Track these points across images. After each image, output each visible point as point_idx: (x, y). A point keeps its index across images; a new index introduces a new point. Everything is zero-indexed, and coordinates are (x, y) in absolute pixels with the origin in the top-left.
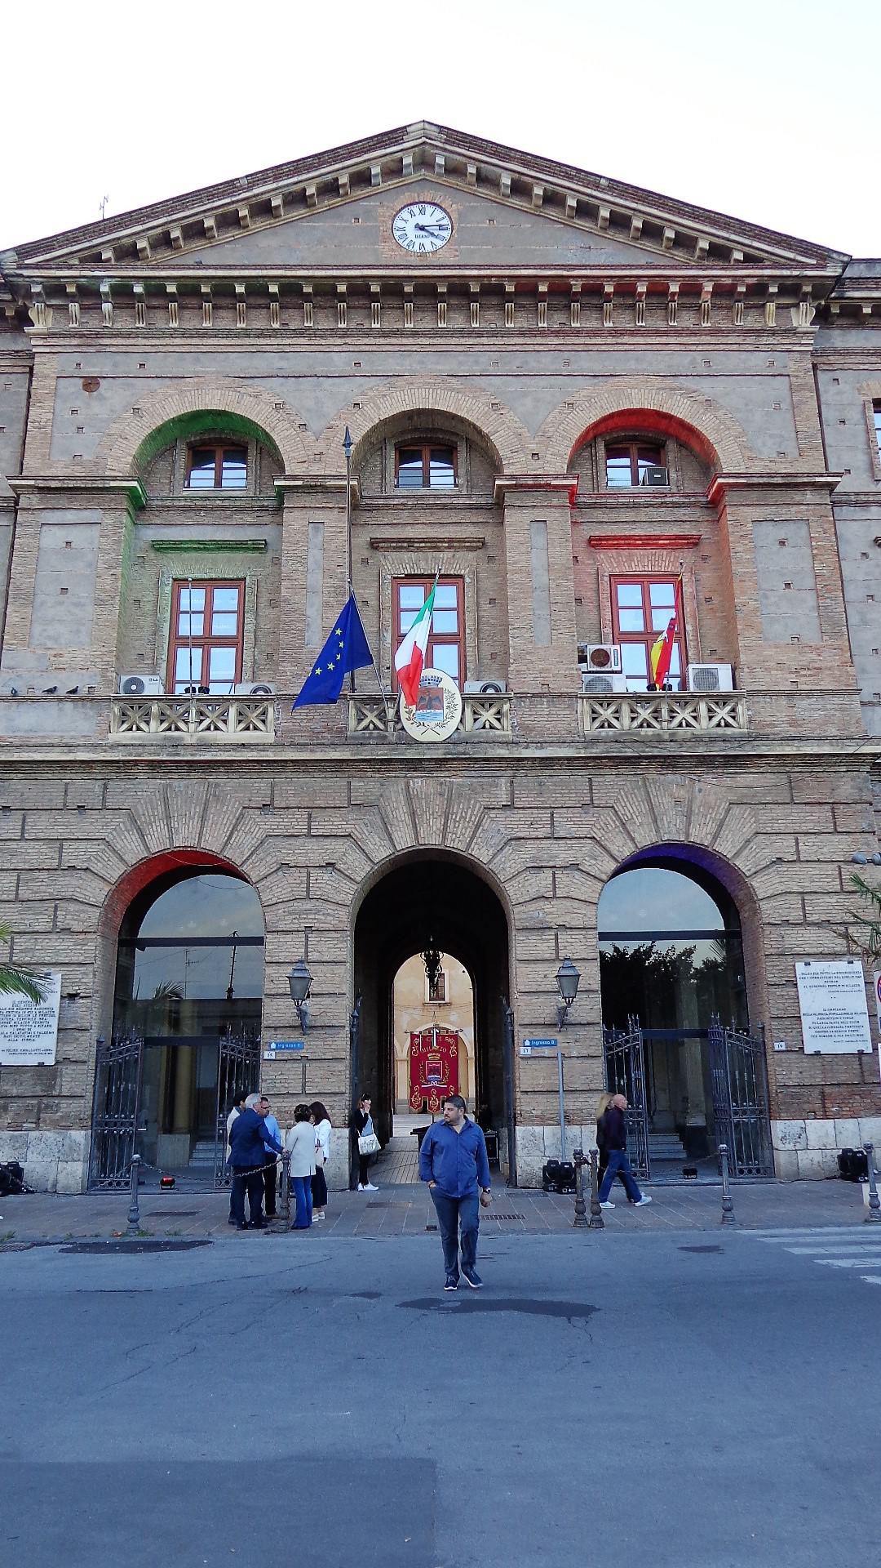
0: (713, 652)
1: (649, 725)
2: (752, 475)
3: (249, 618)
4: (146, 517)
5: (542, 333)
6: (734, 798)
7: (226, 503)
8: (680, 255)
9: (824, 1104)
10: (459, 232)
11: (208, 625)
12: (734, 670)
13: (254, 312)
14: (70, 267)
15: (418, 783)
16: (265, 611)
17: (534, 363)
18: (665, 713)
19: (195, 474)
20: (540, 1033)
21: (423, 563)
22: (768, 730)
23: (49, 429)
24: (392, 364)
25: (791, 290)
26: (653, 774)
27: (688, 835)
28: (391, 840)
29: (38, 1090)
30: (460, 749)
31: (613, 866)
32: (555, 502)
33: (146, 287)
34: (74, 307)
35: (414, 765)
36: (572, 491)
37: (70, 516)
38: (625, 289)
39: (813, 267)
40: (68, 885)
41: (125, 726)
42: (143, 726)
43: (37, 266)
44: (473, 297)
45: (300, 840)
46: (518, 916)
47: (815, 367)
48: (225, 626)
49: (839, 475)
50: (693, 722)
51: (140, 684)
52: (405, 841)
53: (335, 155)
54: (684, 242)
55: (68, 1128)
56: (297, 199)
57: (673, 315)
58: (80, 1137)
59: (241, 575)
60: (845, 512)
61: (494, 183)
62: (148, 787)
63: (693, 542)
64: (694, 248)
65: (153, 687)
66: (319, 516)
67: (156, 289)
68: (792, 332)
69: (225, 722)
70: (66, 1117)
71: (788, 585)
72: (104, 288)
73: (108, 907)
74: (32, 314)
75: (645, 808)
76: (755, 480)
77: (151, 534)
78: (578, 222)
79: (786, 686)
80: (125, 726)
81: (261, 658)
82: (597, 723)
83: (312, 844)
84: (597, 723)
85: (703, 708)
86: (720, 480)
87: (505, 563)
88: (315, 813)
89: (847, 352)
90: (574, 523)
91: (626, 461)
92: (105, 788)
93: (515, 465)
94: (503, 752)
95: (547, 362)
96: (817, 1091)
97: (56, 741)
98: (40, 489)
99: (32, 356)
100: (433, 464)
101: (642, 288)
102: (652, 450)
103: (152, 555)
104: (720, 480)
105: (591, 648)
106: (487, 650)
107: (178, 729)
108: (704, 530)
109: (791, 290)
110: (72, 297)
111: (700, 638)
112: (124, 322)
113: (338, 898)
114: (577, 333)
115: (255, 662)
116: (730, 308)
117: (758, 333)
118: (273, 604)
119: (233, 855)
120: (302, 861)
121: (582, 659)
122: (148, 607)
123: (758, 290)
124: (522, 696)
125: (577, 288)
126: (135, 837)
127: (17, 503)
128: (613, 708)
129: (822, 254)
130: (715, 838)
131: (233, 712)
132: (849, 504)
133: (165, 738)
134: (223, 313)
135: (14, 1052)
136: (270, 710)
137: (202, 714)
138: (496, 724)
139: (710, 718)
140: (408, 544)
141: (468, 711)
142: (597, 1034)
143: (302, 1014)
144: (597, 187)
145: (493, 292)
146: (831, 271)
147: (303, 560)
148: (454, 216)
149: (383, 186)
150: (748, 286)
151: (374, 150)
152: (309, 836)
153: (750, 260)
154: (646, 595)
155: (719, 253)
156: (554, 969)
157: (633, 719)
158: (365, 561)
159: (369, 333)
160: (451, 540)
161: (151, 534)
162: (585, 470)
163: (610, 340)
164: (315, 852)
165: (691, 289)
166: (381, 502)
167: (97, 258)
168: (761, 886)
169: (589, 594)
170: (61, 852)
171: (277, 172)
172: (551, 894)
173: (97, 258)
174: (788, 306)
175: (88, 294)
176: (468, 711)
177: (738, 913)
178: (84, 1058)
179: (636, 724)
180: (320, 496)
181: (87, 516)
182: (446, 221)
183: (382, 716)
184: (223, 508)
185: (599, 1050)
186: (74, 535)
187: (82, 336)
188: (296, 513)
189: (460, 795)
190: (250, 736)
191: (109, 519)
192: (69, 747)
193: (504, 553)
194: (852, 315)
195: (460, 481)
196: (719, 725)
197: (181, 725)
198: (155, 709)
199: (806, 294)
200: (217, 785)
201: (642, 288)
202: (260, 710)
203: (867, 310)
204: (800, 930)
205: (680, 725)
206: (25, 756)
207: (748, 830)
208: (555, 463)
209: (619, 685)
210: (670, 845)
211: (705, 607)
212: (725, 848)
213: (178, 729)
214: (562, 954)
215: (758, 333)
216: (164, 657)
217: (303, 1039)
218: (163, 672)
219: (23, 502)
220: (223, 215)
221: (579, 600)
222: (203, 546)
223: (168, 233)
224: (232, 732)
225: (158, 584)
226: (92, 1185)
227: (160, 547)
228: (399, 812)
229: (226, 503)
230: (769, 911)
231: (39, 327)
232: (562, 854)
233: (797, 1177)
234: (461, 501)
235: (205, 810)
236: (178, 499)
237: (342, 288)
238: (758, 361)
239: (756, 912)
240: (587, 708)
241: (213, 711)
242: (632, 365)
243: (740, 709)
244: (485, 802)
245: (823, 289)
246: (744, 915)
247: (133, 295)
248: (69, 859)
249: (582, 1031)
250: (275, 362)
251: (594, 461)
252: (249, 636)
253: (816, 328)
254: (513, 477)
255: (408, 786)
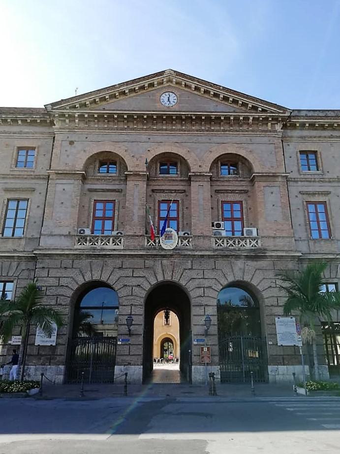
0: (251, 224)
1: (232, 246)
2: (262, 173)
3: (116, 212)
4: (86, 181)
5: (203, 130)
6: (257, 267)
7: (110, 178)
8: (243, 108)
9: (283, 361)
10: (179, 102)
11: (104, 213)
12: (257, 230)
13: (119, 123)
14: (67, 110)
15: (165, 262)
16: (121, 210)
17: (200, 139)
18: (237, 242)
19: (101, 169)
20: (199, 338)
21: (167, 197)
22: (267, 248)
23: (59, 156)
24: (159, 139)
25: (276, 119)
26: (233, 260)
27: (243, 279)
28: (156, 278)
29: (50, 353)
30: (177, 252)
31: (221, 287)
32: (206, 180)
33: (88, 115)
34: (67, 121)
35: (164, 256)
36: (211, 177)
37: (64, 181)
38: (227, 118)
39: (282, 113)
40: (61, 291)
41: (79, 243)
42: (84, 243)
43: (57, 109)
44: (183, 120)
45: (130, 278)
46: (193, 302)
47: (282, 141)
48: (109, 214)
49: (289, 173)
50: (245, 245)
51: (84, 231)
52: (160, 278)
53: (144, 78)
54: (244, 105)
55: (59, 365)
56: (133, 91)
57: (241, 126)
58: (62, 367)
59: (114, 199)
60: (291, 183)
61: (190, 87)
62: (85, 262)
63: (246, 192)
64: (248, 106)
65: (88, 232)
66: (137, 183)
67: (91, 116)
68: (276, 131)
69: (109, 243)
70: (58, 361)
71: (273, 205)
72: (76, 116)
73: (72, 297)
74: (55, 122)
75: (231, 270)
76: (265, 175)
77: (88, 186)
78: (214, 99)
79: (273, 235)
80: (79, 243)
81: (120, 224)
82: (217, 245)
83: (134, 279)
84: (217, 245)
85: (248, 241)
86: (254, 174)
87: (191, 197)
88: (135, 270)
89: (291, 137)
90: (211, 186)
91: (227, 167)
92: (73, 261)
93: (194, 169)
94: (189, 253)
95: (203, 139)
96: (281, 357)
97: (58, 248)
98: (56, 173)
99: (55, 134)
100: (171, 167)
101: (232, 118)
102: (235, 165)
103: (88, 193)
104: (254, 174)
105: (215, 223)
106: (185, 223)
107: (95, 244)
108: (249, 188)
109: (276, 119)
110: (67, 118)
111: (248, 220)
112: (82, 125)
113: (141, 295)
114: (213, 131)
115: (118, 225)
116: (258, 124)
117: (266, 131)
118: (123, 208)
119: (110, 282)
120: (131, 284)
121: (213, 226)
122: (86, 208)
123: (266, 119)
124: (195, 236)
125: (213, 117)
126: (82, 277)
127: (49, 177)
128: (222, 240)
129: (284, 110)
130: (251, 280)
131: (111, 239)
132: (292, 181)
133: (92, 247)
134: (110, 123)
135: (43, 341)
136: (122, 239)
137: (102, 240)
138: (188, 244)
139: (250, 244)
140: (163, 191)
141: (180, 241)
142: (216, 338)
143: (130, 330)
144: (219, 89)
145: (189, 119)
146: (287, 114)
147: (133, 195)
148: (178, 96)
149: (158, 87)
150: (263, 118)
151: (155, 77)
152: (133, 276)
153: (263, 111)
154: (232, 207)
155: (254, 108)
156: (204, 318)
157: (227, 244)
158: (151, 196)
159: (153, 130)
160: (175, 190)
161: (88, 186)
162: (215, 170)
163: (222, 133)
164: (134, 282)
165: (246, 119)
166: (155, 179)
167: (75, 107)
168: (265, 294)
169: (215, 206)
170: (59, 280)
171: (127, 83)
172: (203, 295)
173: (75, 107)
174: (275, 124)
175: (71, 117)
176: (180, 241)
177: (258, 302)
178: (64, 343)
179: (229, 245)
180: (138, 177)
181: (70, 181)
182: (176, 98)
183: (155, 241)
184: (109, 179)
185: (217, 343)
186: (65, 187)
187: (69, 129)
188: (131, 182)
189: (176, 265)
190: (116, 247)
191: (76, 182)
192: (63, 250)
193: (191, 195)
194: (293, 126)
195: (178, 173)
196: (253, 246)
197: (96, 243)
198: (88, 238)
199: (280, 121)
200: (106, 261)
201: (232, 118)
202: (119, 239)
203: (298, 125)
204: (277, 308)
205: (241, 246)
206: (49, 252)
207: (261, 278)
208: (206, 169)
209: (224, 234)
210: (238, 281)
211: (249, 211)
212: (254, 282)
213: (95, 244)
214: (206, 314)
215: (266, 131)
216: (91, 223)
217: (130, 338)
218: (91, 227)
219: (51, 177)
220: (112, 95)
221: (212, 208)
222: (103, 191)
223: (95, 100)
224: (111, 246)
225: (90, 202)
226: (66, 382)
227: (90, 190)
228: (159, 271)
229: (110, 178)
230: (267, 302)
231: (57, 126)
232: (207, 283)
233: (275, 382)
234: (179, 179)
235: (102, 269)
236: (96, 176)
237: (145, 117)
238: (266, 139)
239: (263, 301)
240: (214, 240)
241: (105, 239)
242: (229, 140)
243: (259, 241)
244: (184, 267)
245: (283, 119)
246: (260, 302)
247: (85, 117)
248: (62, 283)
249: (212, 337)
250: (126, 138)
251: (217, 167)
252: (116, 217)
253: (282, 130)
254: (193, 173)
255: (161, 262)
